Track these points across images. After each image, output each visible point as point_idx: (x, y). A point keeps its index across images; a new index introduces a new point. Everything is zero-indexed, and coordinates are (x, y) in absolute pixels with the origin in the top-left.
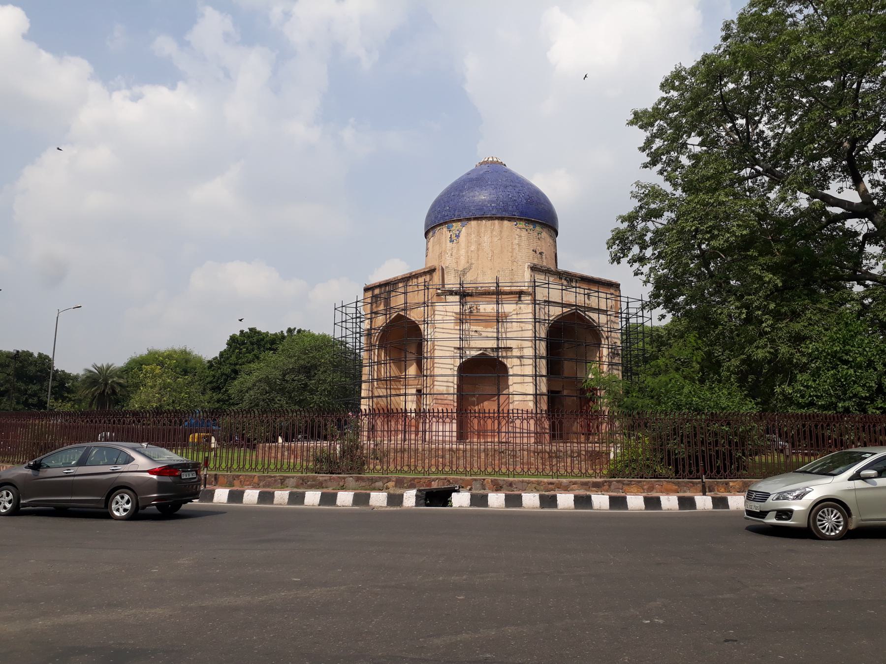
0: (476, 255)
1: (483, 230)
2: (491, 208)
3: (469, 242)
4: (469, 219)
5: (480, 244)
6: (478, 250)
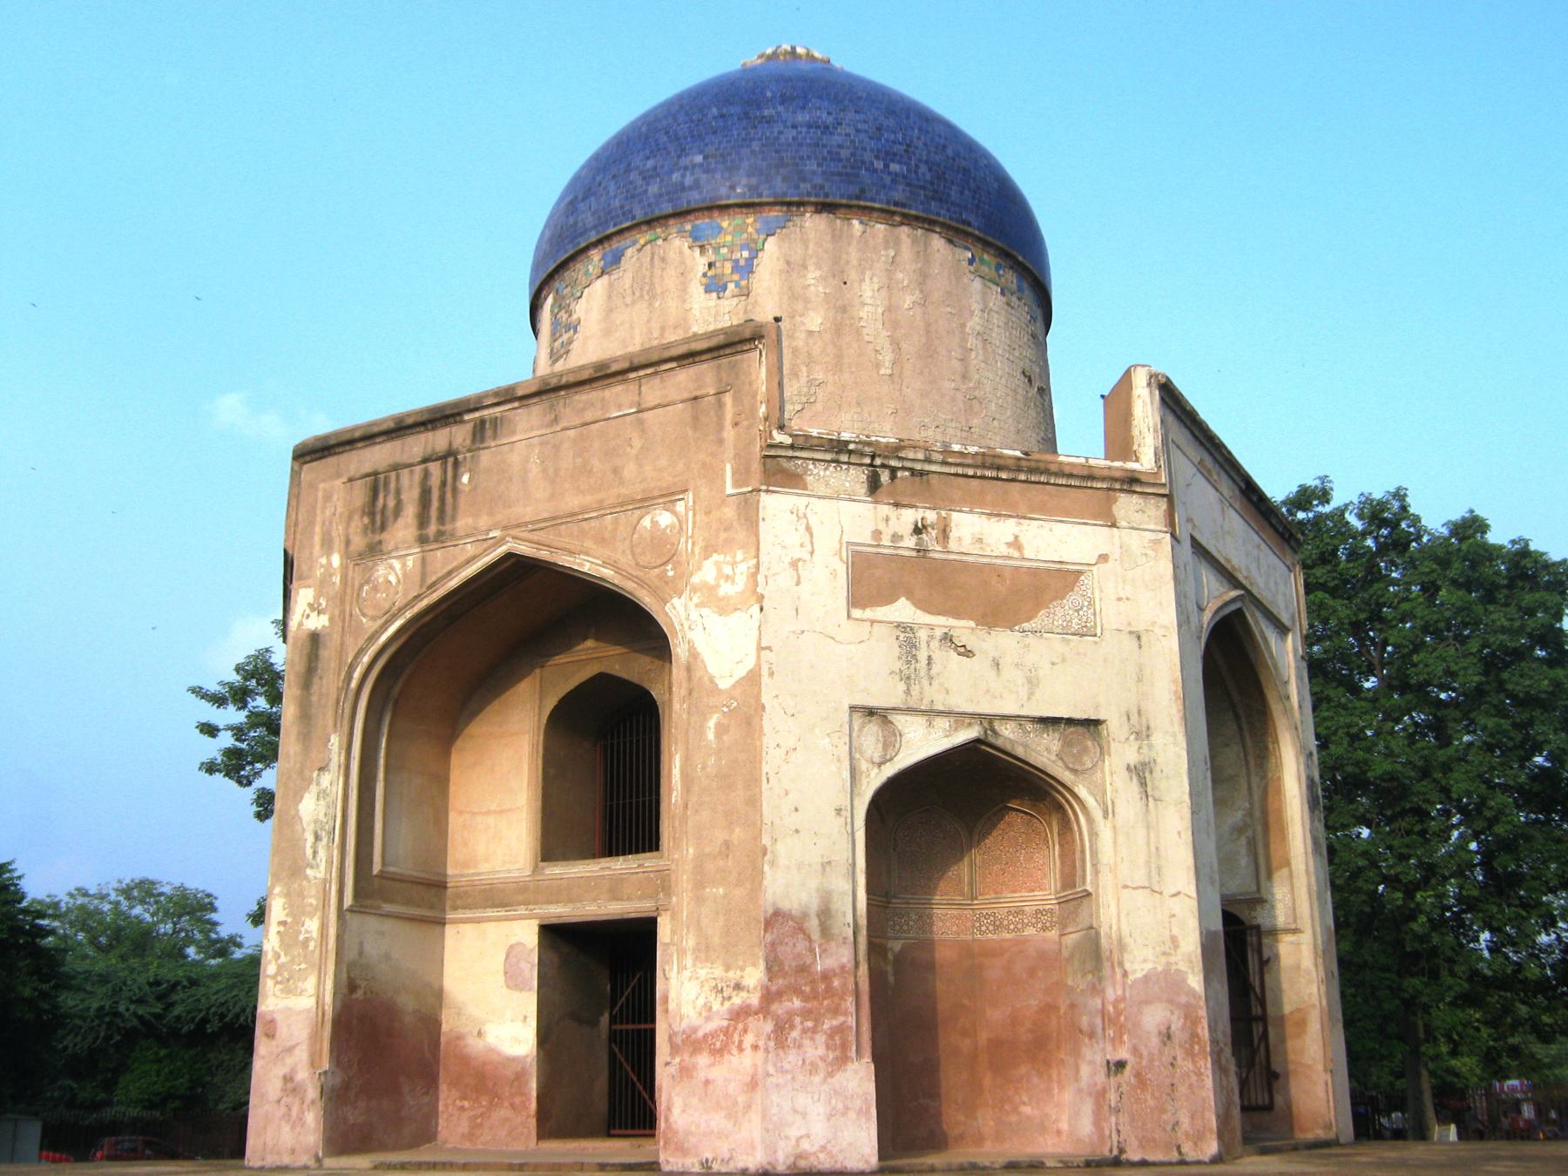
0: (830, 349)
1: (854, 255)
2: (887, 179)
3: (793, 297)
4: (799, 204)
5: (844, 309)
6: (838, 330)
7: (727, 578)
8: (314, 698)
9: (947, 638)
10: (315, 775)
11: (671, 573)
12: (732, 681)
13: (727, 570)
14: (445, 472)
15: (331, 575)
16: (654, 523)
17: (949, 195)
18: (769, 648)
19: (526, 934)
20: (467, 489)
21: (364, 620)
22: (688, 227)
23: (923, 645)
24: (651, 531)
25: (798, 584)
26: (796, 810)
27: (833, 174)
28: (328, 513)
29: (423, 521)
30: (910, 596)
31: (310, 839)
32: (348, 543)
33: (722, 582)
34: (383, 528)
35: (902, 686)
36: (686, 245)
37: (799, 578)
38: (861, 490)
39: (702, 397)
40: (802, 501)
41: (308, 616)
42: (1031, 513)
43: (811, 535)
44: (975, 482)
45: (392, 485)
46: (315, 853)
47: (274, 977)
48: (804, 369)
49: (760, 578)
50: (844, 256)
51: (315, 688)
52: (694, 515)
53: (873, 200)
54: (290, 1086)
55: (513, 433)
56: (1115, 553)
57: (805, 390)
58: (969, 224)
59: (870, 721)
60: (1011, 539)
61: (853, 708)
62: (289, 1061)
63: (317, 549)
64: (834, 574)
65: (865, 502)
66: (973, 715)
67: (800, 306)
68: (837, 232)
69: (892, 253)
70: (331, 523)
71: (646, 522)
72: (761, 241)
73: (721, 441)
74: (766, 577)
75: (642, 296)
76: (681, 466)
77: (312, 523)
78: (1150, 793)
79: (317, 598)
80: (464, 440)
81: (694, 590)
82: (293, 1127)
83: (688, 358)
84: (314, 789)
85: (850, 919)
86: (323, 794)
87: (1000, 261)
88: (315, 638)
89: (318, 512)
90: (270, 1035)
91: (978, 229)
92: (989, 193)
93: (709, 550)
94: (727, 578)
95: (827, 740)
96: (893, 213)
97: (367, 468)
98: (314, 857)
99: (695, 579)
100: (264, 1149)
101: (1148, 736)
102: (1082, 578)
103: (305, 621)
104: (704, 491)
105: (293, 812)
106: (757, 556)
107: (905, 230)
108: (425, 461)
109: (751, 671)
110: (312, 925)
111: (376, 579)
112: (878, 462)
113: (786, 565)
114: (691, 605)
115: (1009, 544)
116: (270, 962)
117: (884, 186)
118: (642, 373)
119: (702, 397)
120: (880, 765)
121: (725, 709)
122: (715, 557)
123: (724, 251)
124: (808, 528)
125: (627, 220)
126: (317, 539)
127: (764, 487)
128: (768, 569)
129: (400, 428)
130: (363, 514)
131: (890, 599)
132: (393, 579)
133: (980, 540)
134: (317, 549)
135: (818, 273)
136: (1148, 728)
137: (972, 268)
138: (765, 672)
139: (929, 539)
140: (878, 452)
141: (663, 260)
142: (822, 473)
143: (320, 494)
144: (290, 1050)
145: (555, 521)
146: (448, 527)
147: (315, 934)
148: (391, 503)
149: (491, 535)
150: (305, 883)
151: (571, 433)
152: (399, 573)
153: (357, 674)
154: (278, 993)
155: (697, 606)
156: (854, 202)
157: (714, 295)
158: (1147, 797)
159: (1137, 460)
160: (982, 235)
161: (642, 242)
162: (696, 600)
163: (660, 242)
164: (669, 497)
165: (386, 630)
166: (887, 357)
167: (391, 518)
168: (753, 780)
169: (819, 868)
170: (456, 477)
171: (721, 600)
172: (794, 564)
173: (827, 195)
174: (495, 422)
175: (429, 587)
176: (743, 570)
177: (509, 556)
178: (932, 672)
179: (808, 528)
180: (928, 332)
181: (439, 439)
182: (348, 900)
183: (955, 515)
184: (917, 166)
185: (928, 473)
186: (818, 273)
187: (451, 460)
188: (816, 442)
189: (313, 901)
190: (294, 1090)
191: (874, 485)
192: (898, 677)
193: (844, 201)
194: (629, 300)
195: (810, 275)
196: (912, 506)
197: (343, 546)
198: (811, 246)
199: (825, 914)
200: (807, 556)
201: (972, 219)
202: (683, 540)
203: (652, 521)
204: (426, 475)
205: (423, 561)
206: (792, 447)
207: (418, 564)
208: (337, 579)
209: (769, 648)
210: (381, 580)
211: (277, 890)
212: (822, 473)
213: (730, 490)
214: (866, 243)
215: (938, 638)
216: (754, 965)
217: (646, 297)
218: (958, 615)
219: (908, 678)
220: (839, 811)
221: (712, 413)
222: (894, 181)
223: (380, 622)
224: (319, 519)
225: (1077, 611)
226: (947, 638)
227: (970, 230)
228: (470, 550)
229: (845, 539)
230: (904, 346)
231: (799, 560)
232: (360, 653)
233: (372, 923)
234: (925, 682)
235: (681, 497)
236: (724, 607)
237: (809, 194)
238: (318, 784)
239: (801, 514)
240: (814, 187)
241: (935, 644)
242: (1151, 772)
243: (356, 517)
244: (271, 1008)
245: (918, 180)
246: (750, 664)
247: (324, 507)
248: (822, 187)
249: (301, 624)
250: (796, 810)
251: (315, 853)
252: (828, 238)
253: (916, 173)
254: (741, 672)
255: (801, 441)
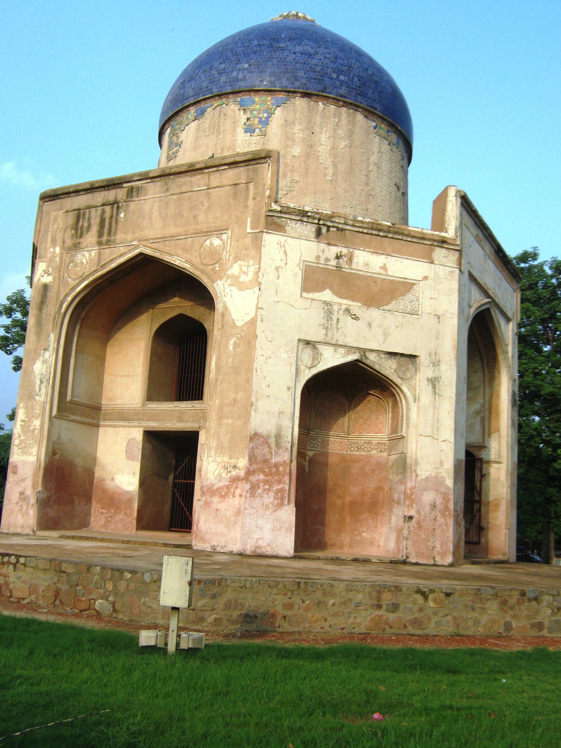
1: (318, 119)
2: (338, 83)
3: (287, 138)
4: (294, 92)
5: (311, 146)
6: (308, 156)
7: (245, 273)
8: (44, 316)
9: (347, 310)
10: (42, 352)
11: (217, 269)
12: (243, 323)
13: (245, 269)
14: (112, 211)
15: (55, 257)
16: (212, 244)
17: (367, 94)
18: (262, 308)
19: (138, 435)
20: (123, 220)
21: (70, 280)
22: (239, 99)
23: (336, 313)
24: (209, 247)
25: (278, 278)
26: (269, 386)
27: (311, 78)
28: (55, 227)
29: (100, 234)
30: (331, 289)
31: (38, 382)
32: (64, 242)
33: (242, 275)
34: (81, 236)
35: (324, 332)
36: (237, 108)
37: (279, 275)
38: (313, 235)
39: (239, 184)
40: (284, 238)
41: (43, 276)
42: (393, 252)
43: (286, 255)
44: (367, 236)
45: (87, 216)
46: (40, 389)
47: (18, 446)
48: (290, 174)
49: (260, 274)
50: (314, 120)
51: (44, 311)
52: (231, 241)
53: (330, 93)
54: (22, 496)
55: (147, 195)
56: (431, 276)
57: (289, 184)
58: (376, 109)
59: (307, 347)
60: (382, 265)
61: (299, 340)
62: (23, 485)
63: (49, 244)
64: (296, 275)
65: (313, 241)
66: (356, 348)
67: (290, 143)
68: (311, 108)
69: (337, 120)
70: (56, 232)
71: (208, 243)
72: (273, 109)
73: (246, 206)
74: (263, 274)
75: (213, 132)
76: (226, 217)
77: (47, 232)
78: (437, 392)
79: (47, 267)
80: (123, 196)
81: (228, 277)
82: (23, 516)
83: (234, 164)
84: (41, 358)
85: (290, 439)
86: (45, 362)
87: (389, 128)
88: (45, 287)
89: (50, 226)
90: (15, 473)
91: (380, 112)
92: (387, 94)
93: (237, 258)
94: (245, 273)
95: (286, 354)
96: (339, 100)
97: (75, 206)
98: (39, 391)
99: (229, 272)
100: (9, 525)
101: (438, 365)
102: (415, 287)
103: (41, 279)
104: (236, 230)
105: (31, 369)
106: (260, 264)
107: (344, 108)
108: (103, 205)
109: (252, 319)
110: (37, 423)
111: (76, 261)
112: (321, 222)
113: (273, 269)
114: (226, 284)
115: (381, 268)
116: (16, 439)
117: (336, 87)
118: (211, 170)
119: (239, 184)
120: (310, 368)
121: (239, 336)
122: (239, 262)
123: (255, 112)
124: (285, 252)
125: (209, 94)
126: (49, 239)
127: (265, 231)
128: (265, 270)
129: (92, 188)
130: (72, 228)
131: (322, 289)
132: (84, 261)
133: (367, 265)
134: (49, 244)
135: (300, 128)
136: (439, 361)
137: (375, 131)
138: (259, 320)
139: (343, 262)
140: (322, 218)
141: (225, 115)
142: (294, 226)
143: (52, 218)
144: (23, 480)
145: (164, 239)
146: (112, 238)
147: (38, 427)
148: (86, 224)
149: (133, 244)
150: (34, 403)
151: (175, 197)
152: (88, 258)
153: (65, 306)
154: (19, 453)
155: (229, 285)
156: (321, 93)
157: (249, 134)
158: (435, 394)
159: (446, 232)
160: (382, 115)
161: (216, 105)
162: (229, 282)
163: (224, 106)
164: (219, 231)
165: (80, 285)
166: (330, 172)
167: (85, 232)
168: (250, 370)
169: (277, 414)
170: (118, 214)
171: (240, 283)
172: (277, 269)
173: (307, 89)
174: (138, 189)
175: (102, 266)
176: (252, 270)
177: (141, 254)
178: (339, 326)
179: (285, 252)
180: (351, 161)
181: (111, 195)
182: (54, 413)
183: (356, 252)
184: (353, 78)
185: (345, 230)
186: (300, 128)
187: (116, 205)
188: (292, 210)
189: (38, 412)
190: (25, 499)
191: (318, 233)
192: (322, 327)
193: (316, 93)
194: (207, 133)
195: (296, 128)
196: (336, 245)
197: (61, 244)
198: (298, 114)
199: (278, 436)
200: (283, 266)
201: (377, 106)
202: (224, 253)
203: (210, 243)
204: (103, 212)
205: (100, 253)
206: (281, 212)
207: (97, 255)
208: (58, 259)
209: (262, 308)
210: (78, 261)
211: (21, 405)
212: (294, 226)
213: (249, 230)
214: (325, 114)
215: (343, 310)
216: (243, 457)
217: (216, 133)
218: (353, 300)
219: (327, 328)
220: (289, 388)
221: (243, 192)
222: (341, 85)
223: (77, 281)
224: (51, 230)
225: (411, 302)
226: (347, 310)
227: (376, 112)
228: (122, 250)
229: (302, 259)
230: (338, 166)
231: (280, 267)
232: (67, 295)
233: (65, 424)
234: (335, 331)
235: (225, 232)
236: (242, 287)
237: (299, 88)
238: (43, 356)
239: (282, 245)
240: (302, 84)
241: (341, 312)
242: (438, 382)
243: (69, 230)
244: (16, 460)
245: (353, 85)
246: (252, 315)
247: (53, 224)
248: (305, 85)
249: (39, 280)
250: (269, 386)
251: (40, 389)
252: (306, 110)
253: (352, 81)
254: (248, 319)
255: (285, 210)
